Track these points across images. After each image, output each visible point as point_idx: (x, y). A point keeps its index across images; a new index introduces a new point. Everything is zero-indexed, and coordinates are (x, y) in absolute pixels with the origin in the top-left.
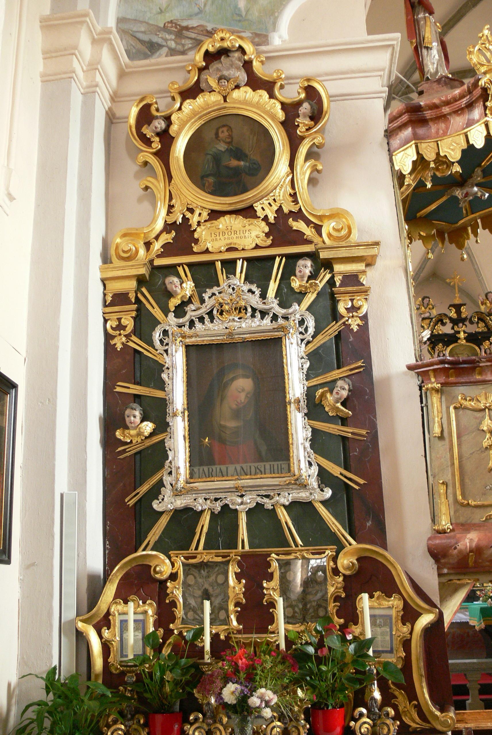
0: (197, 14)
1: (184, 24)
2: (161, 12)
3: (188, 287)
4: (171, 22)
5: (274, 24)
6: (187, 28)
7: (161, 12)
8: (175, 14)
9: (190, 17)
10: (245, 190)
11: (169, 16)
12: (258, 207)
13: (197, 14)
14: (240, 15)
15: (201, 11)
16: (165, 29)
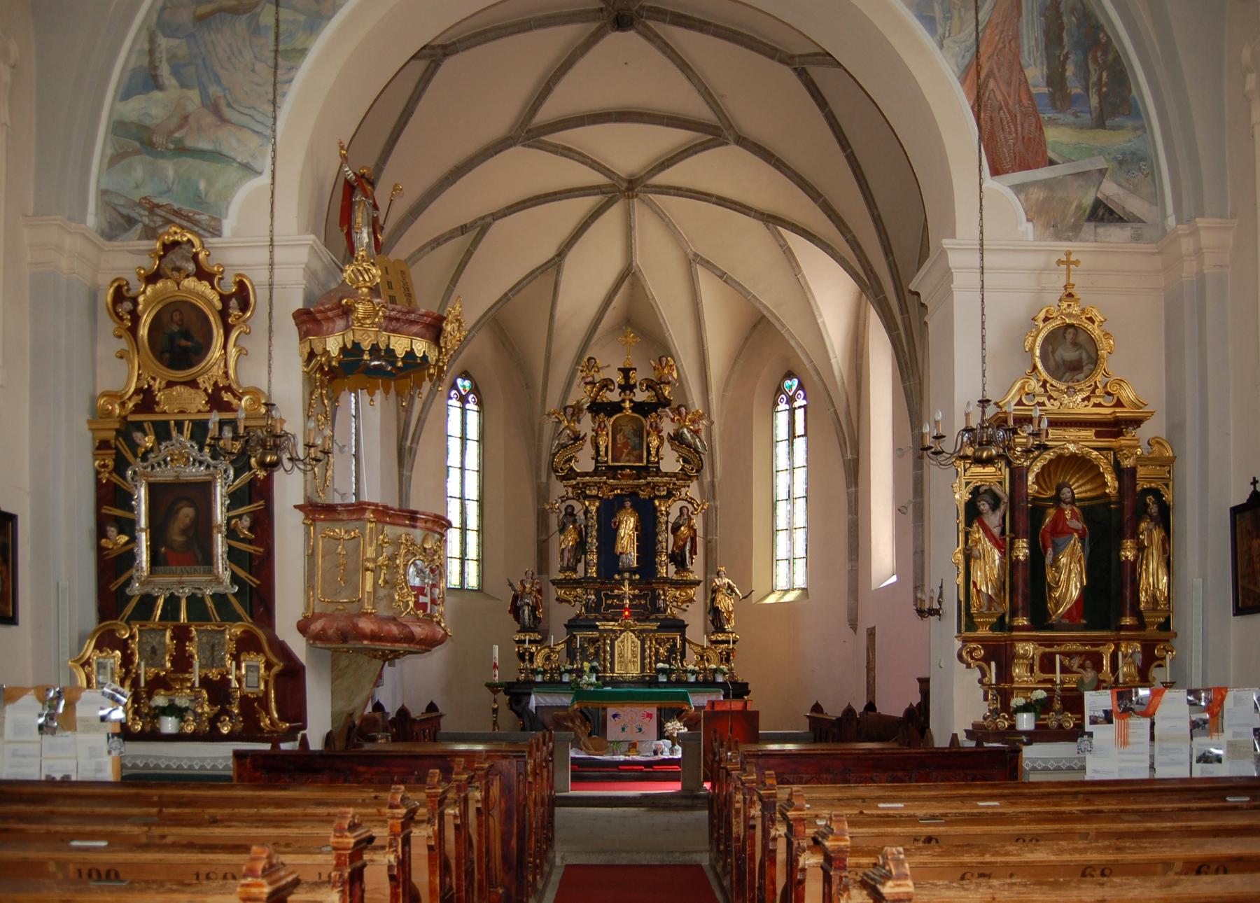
0: (166, 192)
1: (156, 201)
2: (137, 187)
3: (149, 441)
4: (145, 198)
5: (227, 208)
6: (158, 206)
7: (137, 187)
8: (146, 191)
9: (161, 194)
10: (191, 366)
11: (144, 192)
12: (200, 380)
13: (166, 192)
14: (200, 197)
15: (169, 190)
16: (140, 204)
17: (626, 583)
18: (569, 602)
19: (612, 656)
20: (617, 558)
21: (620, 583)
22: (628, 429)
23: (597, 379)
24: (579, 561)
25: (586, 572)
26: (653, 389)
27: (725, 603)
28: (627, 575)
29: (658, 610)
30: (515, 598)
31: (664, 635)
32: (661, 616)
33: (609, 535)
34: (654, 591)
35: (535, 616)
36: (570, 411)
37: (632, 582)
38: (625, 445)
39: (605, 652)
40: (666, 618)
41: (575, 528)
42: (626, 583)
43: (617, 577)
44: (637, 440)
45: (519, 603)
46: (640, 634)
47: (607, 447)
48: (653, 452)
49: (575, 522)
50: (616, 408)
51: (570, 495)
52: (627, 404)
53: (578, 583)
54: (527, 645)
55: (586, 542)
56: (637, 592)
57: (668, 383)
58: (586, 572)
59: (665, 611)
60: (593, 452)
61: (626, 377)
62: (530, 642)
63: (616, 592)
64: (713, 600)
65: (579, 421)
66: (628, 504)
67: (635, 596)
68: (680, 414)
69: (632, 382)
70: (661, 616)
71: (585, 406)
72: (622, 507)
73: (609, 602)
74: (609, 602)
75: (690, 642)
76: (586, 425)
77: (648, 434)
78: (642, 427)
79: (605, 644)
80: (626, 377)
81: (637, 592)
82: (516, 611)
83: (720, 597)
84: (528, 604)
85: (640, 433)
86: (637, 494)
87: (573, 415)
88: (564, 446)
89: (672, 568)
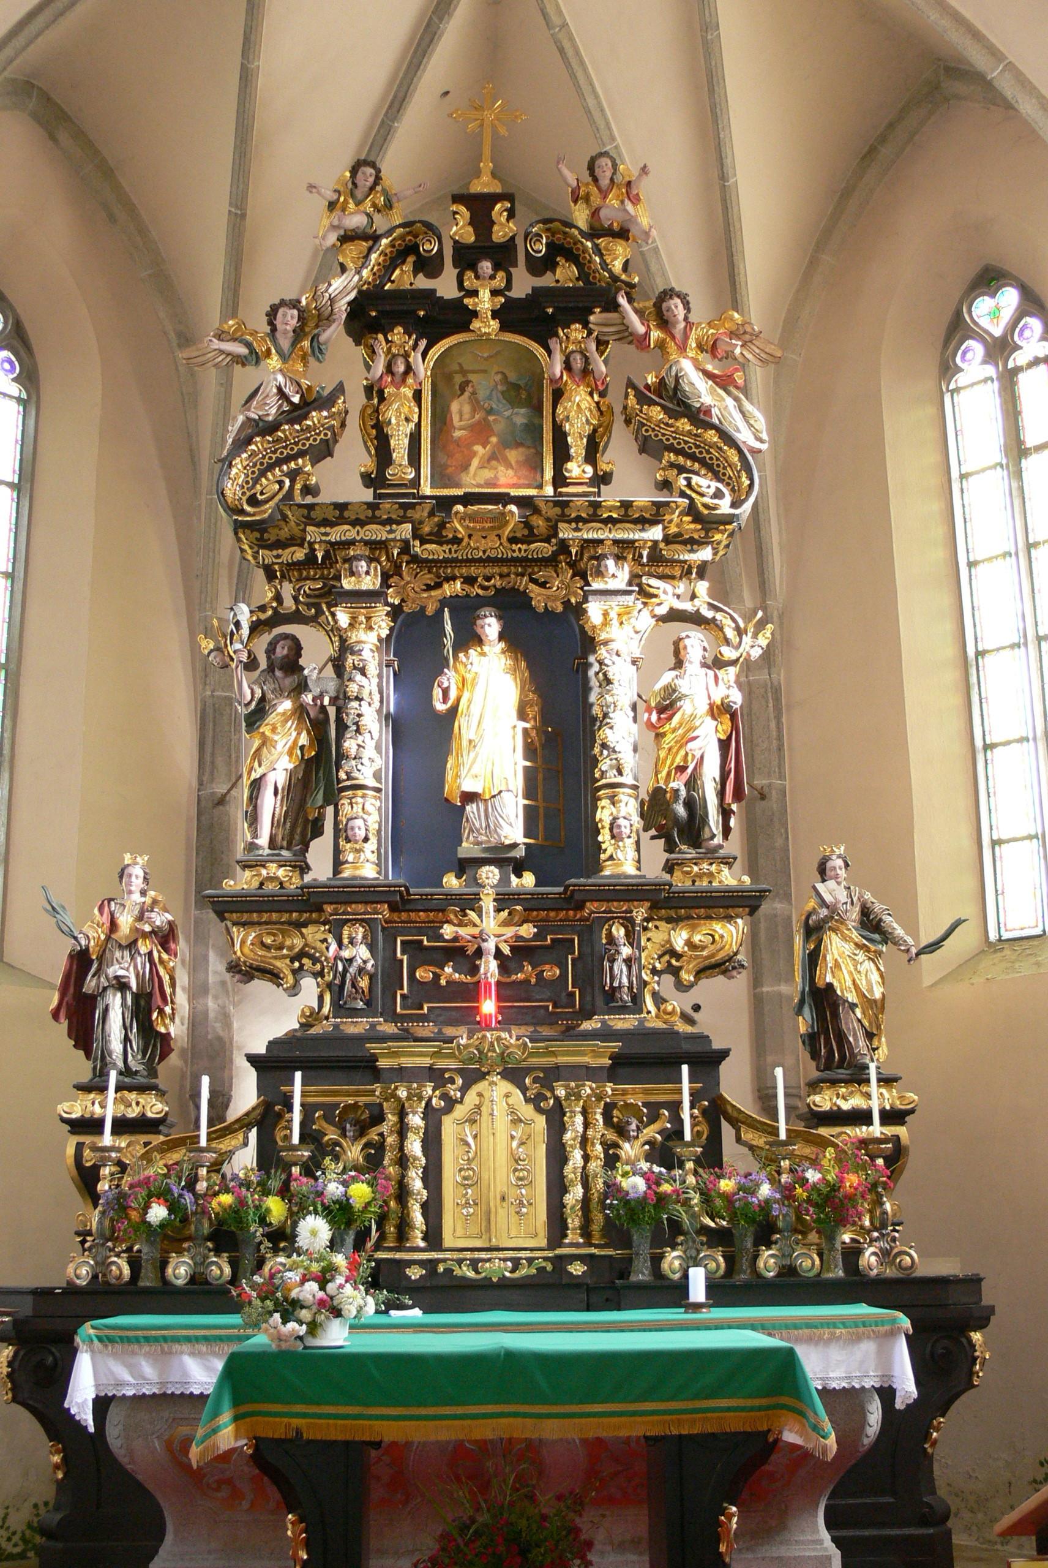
17: (488, 903)
18: (274, 976)
19: (433, 1176)
20: (452, 812)
21: (469, 902)
22: (485, 384)
23: (381, 223)
24: (318, 832)
25: (338, 864)
26: (573, 256)
27: (850, 968)
28: (490, 875)
29: (610, 999)
30: (80, 962)
31: (636, 1095)
32: (623, 1023)
33: (425, 735)
34: (589, 929)
35: (147, 1031)
36: (289, 319)
37: (504, 901)
38: (481, 431)
39: (403, 1161)
40: (642, 1034)
41: (300, 711)
42: (488, 903)
43: (452, 882)
44: (521, 416)
45: (90, 984)
46: (538, 1082)
47: (415, 439)
48: (577, 447)
49: (302, 686)
50: (444, 319)
51: (289, 604)
52: (485, 302)
53: (312, 904)
54: (107, 1139)
55: (341, 756)
56: (528, 930)
57: (622, 234)
58: (338, 864)
59: (637, 1000)
60: (367, 463)
61: (482, 221)
62: (121, 1126)
63: (448, 931)
64: (813, 959)
65: (318, 350)
66: (491, 627)
67: (522, 951)
68: (664, 322)
69: (501, 232)
70: (623, 1023)
71: (342, 306)
72: (468, 638)
73: (424, 974)
74: (424, 974)
75: (738, 1121)
76: (345, 363)
77: (558, 395)
78: (536, 376)
79: (402, 1131)
80: (482, 221)
81: (528, 930)
82: (80, 1015)
83: (838, 948)
84: (122, 985)
85: (532, 395)
86: (524, 600)
87: (299, 333)
88: (269, 429)
89: (656, 853)
